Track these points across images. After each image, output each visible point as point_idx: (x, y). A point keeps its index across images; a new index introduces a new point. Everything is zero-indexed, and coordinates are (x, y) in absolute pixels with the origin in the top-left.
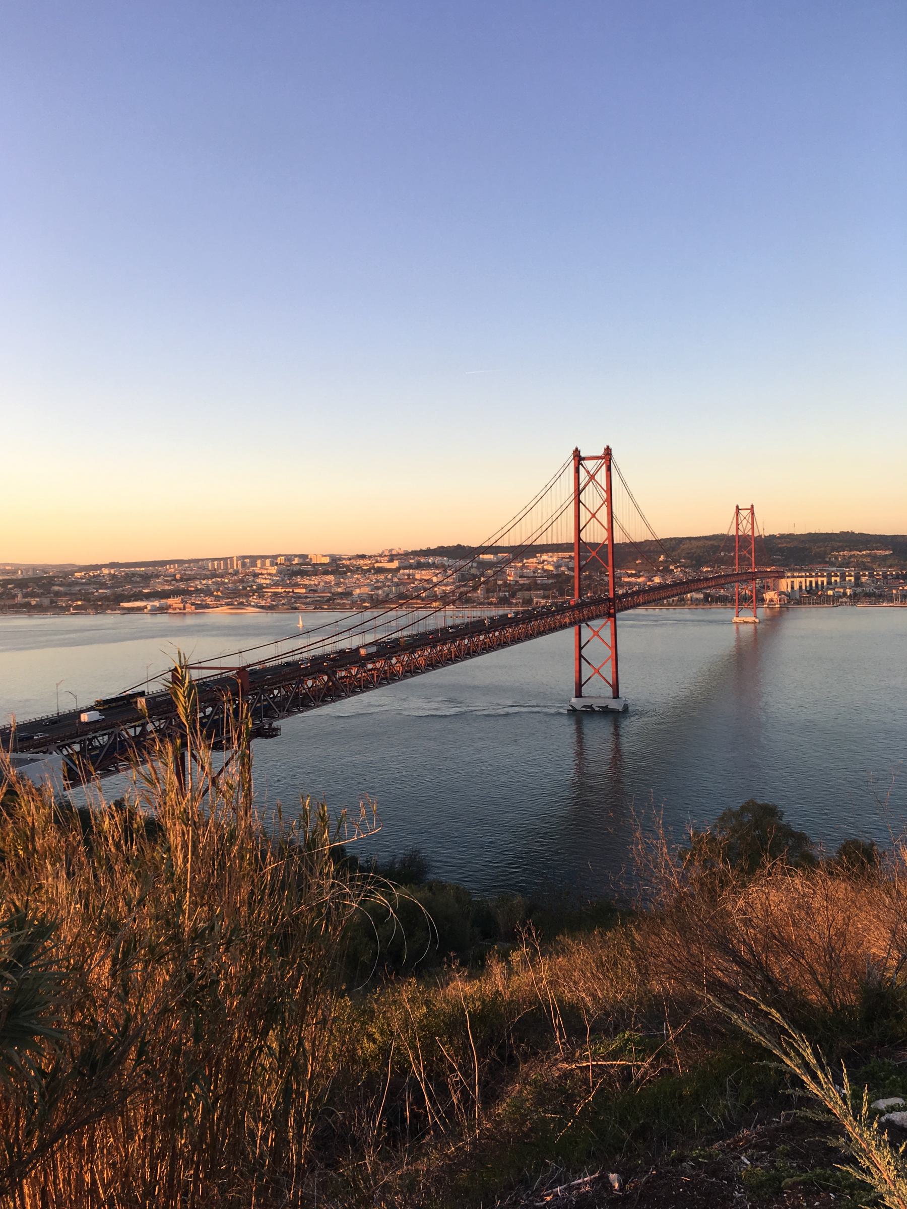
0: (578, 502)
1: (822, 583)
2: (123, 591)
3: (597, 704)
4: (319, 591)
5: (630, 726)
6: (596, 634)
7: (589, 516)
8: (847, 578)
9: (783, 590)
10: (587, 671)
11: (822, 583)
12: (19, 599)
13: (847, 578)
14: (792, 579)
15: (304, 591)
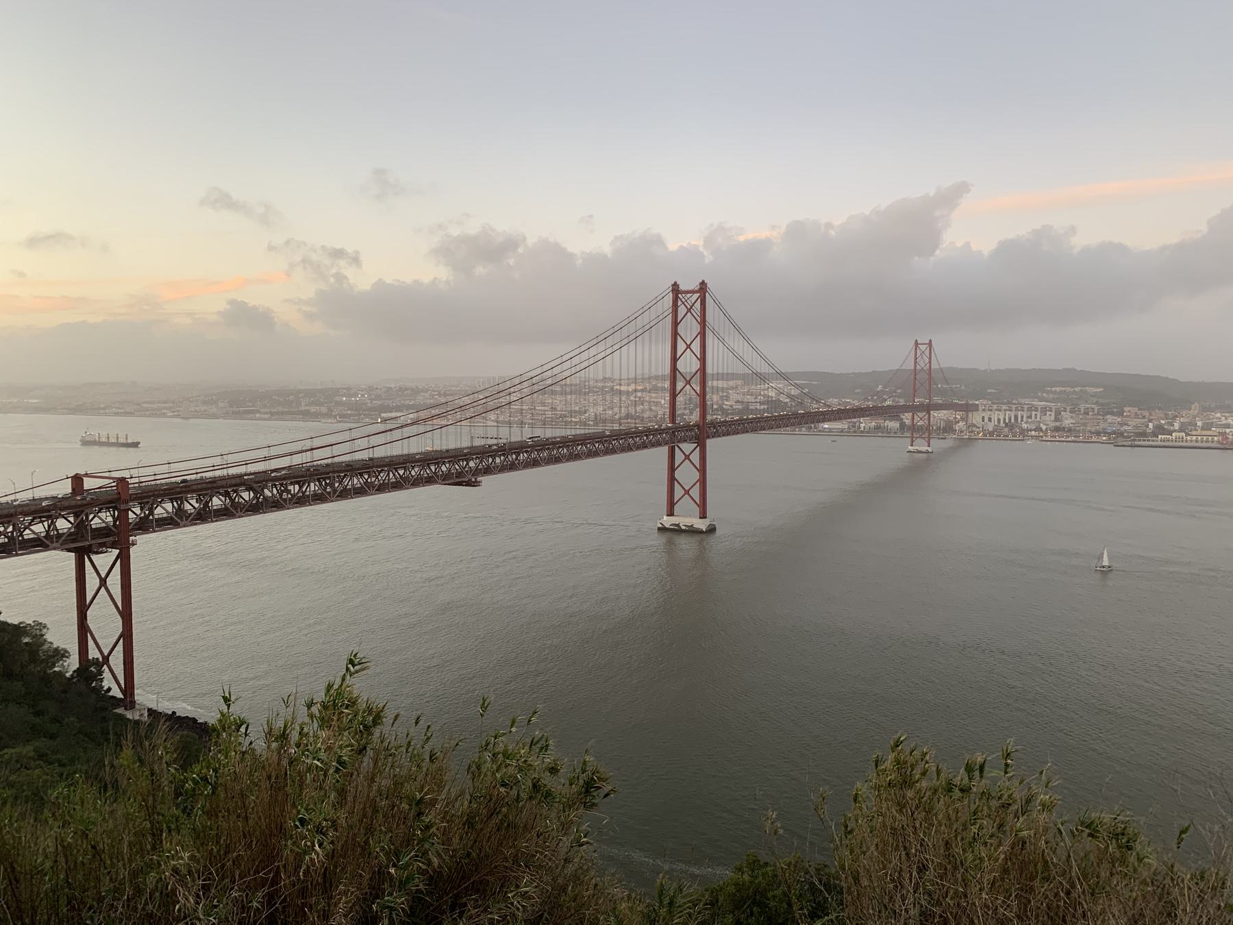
0: (675, 334)
1: (1022, 417)
2: (393, 402)
3: (683, 521)
4: (558, 409)
5: (716, 544)
6: (687, 457)
7: (685, 347)
8: (1048, 413)
9: (974, 422)
10: (678, 492)
11: (1022, 417)
12: (303, 408)
13: (1048, 413)
14: (989, 413)
15: (546, 408)
